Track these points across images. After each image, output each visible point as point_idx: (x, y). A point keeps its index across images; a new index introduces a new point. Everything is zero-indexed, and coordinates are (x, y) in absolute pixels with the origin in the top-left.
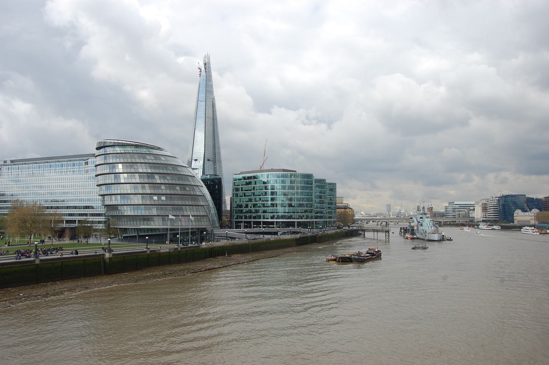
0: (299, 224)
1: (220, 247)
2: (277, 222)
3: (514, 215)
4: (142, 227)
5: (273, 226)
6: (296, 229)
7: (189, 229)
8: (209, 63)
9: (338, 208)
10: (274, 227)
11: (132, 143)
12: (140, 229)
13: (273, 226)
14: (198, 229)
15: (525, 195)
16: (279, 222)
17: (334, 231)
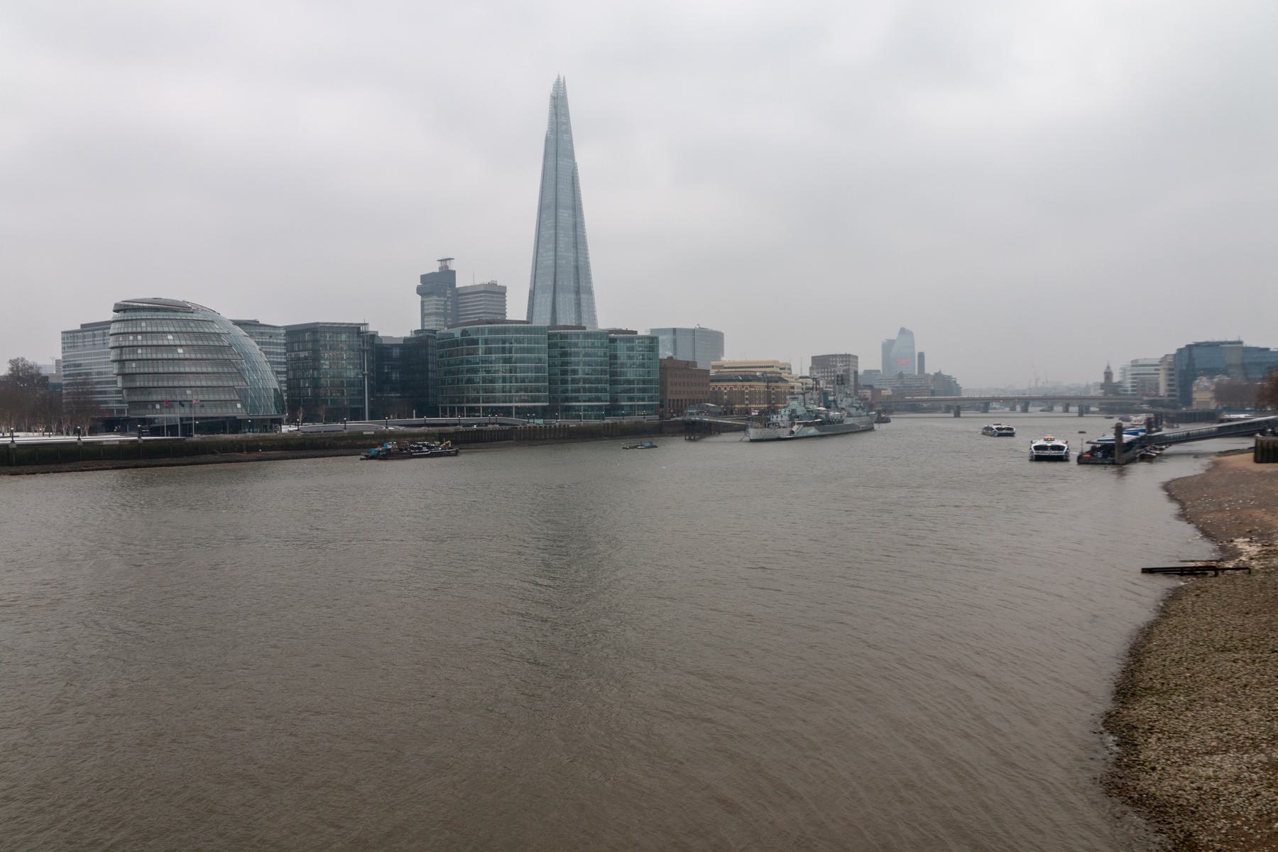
0: (521, 412)
1: (232, 442)
2: (483, 407)
3: (1194, 389)
4: (148, 416)
5: (478, 414)
6: (513, 419)
7: (191, 418)
8: (564, 98)
9: (712, 381)
10: (479, 416)
11: (145, 305)
12: (147, 418)
13: (478, 414)
14: (227, 418)
15: (1240, 343)
16: (488, 407)
17: (598, 422)
